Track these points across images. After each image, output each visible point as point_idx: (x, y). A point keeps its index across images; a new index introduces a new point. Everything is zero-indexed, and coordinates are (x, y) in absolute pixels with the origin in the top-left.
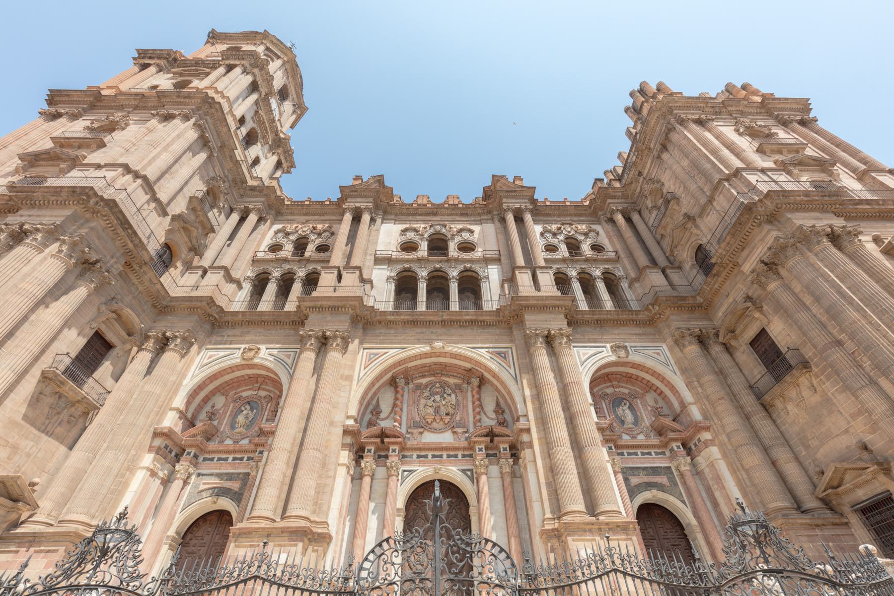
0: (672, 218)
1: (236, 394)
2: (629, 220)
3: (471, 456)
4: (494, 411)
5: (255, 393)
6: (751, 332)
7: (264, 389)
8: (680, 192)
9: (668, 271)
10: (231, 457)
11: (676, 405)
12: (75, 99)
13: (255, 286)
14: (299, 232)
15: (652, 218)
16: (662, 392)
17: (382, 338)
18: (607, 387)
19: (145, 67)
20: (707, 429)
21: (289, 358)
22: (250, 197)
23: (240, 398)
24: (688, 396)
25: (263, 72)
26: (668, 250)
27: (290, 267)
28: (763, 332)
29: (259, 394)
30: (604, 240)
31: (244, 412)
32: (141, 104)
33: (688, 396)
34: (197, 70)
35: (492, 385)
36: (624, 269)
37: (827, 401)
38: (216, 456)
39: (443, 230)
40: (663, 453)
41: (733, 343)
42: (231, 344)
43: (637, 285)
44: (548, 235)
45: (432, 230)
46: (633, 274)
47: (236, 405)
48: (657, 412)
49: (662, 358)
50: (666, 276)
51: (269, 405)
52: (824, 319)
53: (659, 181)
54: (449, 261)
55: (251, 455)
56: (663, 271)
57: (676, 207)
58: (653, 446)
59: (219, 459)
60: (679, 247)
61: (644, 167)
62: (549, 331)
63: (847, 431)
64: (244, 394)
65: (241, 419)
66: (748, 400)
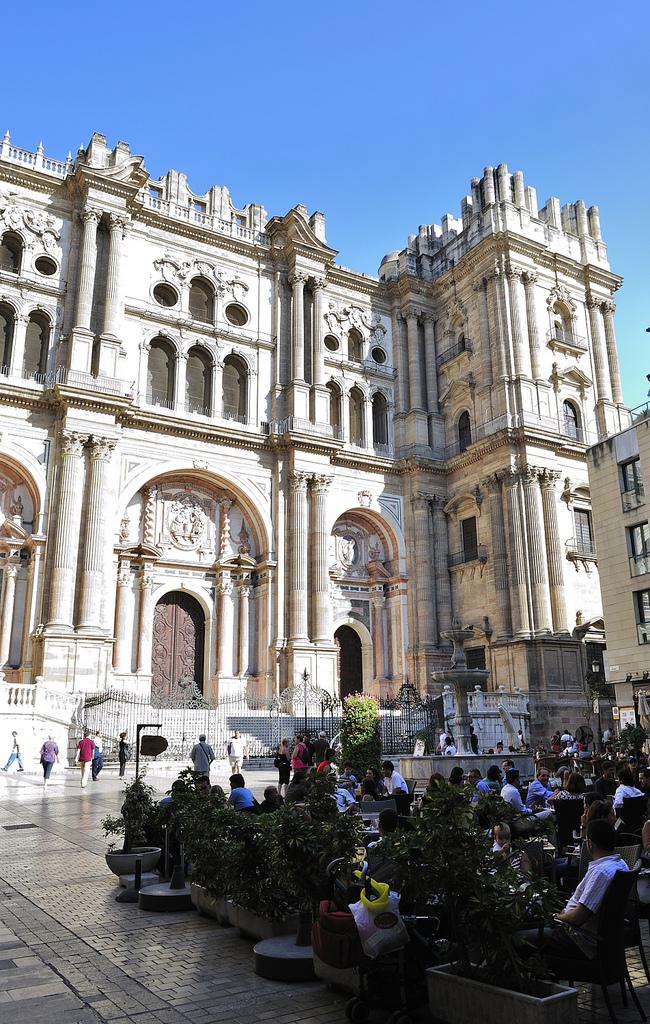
0: (459, 364)
2: (421, 326)
3: (214, 576)
4: (239, 535)
6: (466, 515)
8: (476, 346)
9: (434, 420)
11: (391, 553)
14: (8, 221)
15: (445, 344)
16: (384, 538)
17: (141, 443)
18: (342, 524)
20: (405, 581)
24: (402, 550)
26: (442, 397)
28: (473, 519)
30: (388, 348)
33: (402, 550)
35: (242, 508)
36: (396, 392)
37: (483, 586)
39: (210, 275)
40: (367, 590)
41: (452, 516)
43: (401, 423)
44: (332, 319)
45: (192, 272)
46: (402, 409)
48: (374, 555)
49: (396, 511)
50: (429, 425)
52: (507, 536)
53: (465, 312)
54: (214, 334)
56: (429, 418)
57: (466, 358)
58: (362, 584)
60: (452, 400)
61: (459, 279)
62: (314, 476)
63: (483, 607)
66: (442, 565)
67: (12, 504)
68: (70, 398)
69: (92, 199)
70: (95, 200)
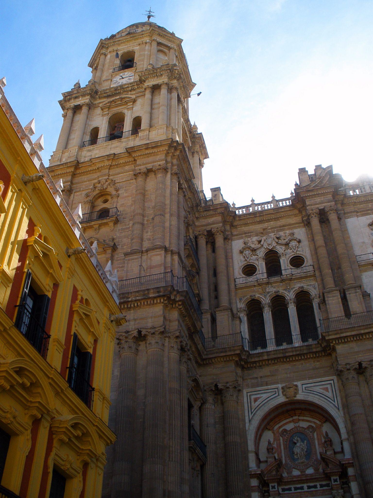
1: (280, 427)
5: (297, 425)
7: (303, 420)
10: (305, 486)
12: (59, 172)
13: (247, 315)
14: (265, 246)
19: (77, 109)
21: (328, 391)
22: (206, 217)
23: (285, 430)
25: (181, 81)
27: (274, 290)
29: (301, 426)
31: (298, 444)
32: (114, 163)
34: (122, 99)
38: (292, 487)
42: (267, 384)
47: (285, 437)
51: (315, 434)
55: (324, 483)
59: (296, 489)
64: (290, 427)
65: (297, 450)
67: (323, 440)
68: (335, 339)
69: (309, 205)
70: (311, 205)
